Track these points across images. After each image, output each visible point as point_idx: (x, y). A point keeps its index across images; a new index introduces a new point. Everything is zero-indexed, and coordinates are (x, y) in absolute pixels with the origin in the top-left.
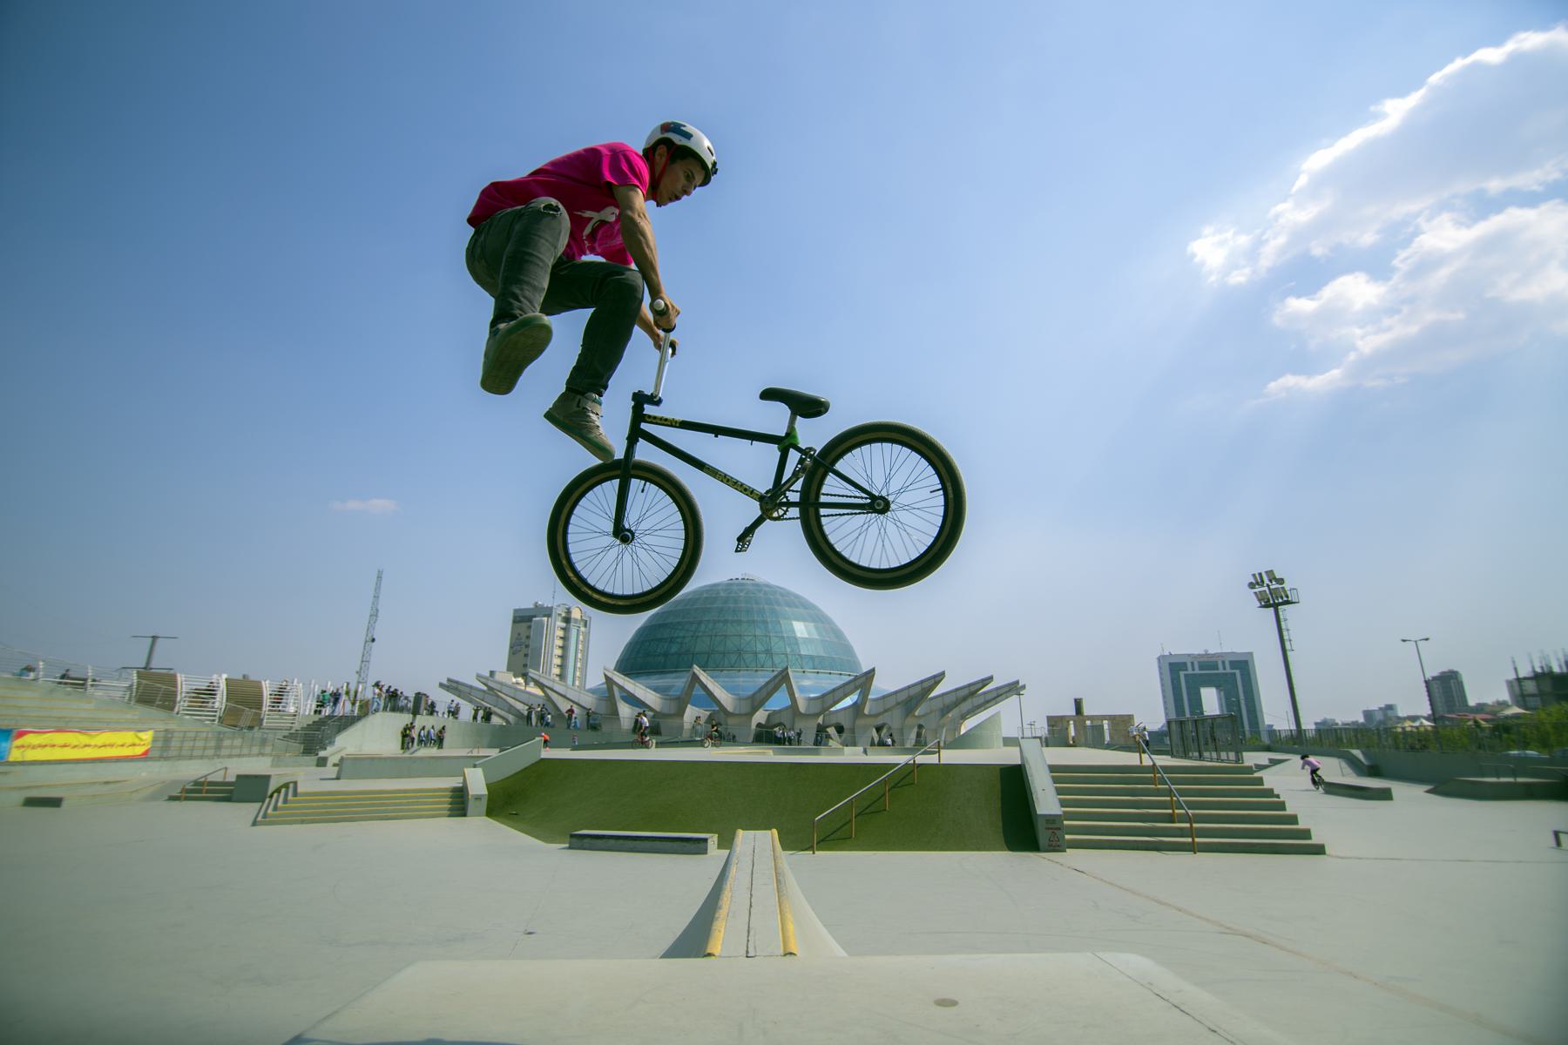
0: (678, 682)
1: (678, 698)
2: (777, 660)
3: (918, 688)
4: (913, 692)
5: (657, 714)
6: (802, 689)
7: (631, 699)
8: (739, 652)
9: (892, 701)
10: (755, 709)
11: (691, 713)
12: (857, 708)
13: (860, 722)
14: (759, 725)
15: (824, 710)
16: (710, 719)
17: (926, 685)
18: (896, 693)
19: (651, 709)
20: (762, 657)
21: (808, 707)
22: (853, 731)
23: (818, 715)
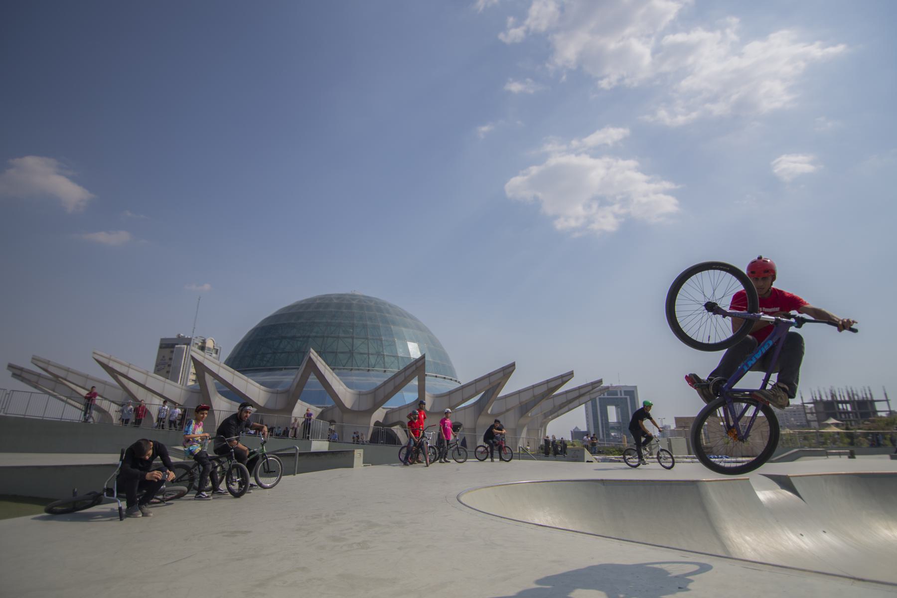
0: (288, 378)
1: (287, 392)
2: (386, 359)
5: (260, 409)
7: (231, 392)
8: (351, 353)
9: (515, 402)
11: (300, 409)
19: (253, 404)
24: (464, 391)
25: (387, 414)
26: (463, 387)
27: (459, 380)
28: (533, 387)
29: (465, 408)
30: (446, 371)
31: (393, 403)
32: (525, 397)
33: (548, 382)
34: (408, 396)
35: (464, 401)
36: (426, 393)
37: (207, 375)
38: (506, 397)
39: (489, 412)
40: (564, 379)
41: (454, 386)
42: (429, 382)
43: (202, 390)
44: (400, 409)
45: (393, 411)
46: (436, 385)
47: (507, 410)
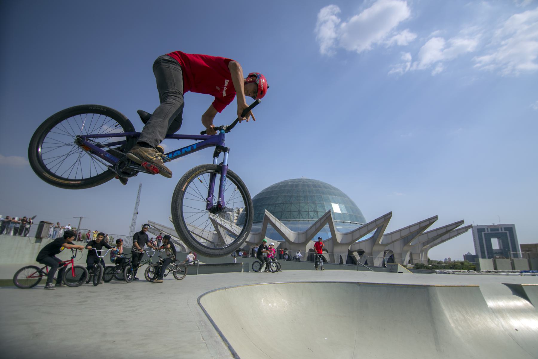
3: (417, 227)
4: (413, 230)
6: (338, 230)
9: (397, 236)
10: (307, 241)
12: (374, 240)
13: (376, 248)
14: (311, 250)
15: (352, 242)
16: (280, 246)
17: (423, 225)
18: (400, 230)
20: (312, 214)
21: (342, 240)
22: (371, 254)
23: (348, 244)
28: (410, 227)
29: (365, 241)
32: (404, 234)
33: (420, 223)
37: (219, 227)
38: (391, 234)
39: (380, 242)
43: (219, 234)
47: (393, 242)
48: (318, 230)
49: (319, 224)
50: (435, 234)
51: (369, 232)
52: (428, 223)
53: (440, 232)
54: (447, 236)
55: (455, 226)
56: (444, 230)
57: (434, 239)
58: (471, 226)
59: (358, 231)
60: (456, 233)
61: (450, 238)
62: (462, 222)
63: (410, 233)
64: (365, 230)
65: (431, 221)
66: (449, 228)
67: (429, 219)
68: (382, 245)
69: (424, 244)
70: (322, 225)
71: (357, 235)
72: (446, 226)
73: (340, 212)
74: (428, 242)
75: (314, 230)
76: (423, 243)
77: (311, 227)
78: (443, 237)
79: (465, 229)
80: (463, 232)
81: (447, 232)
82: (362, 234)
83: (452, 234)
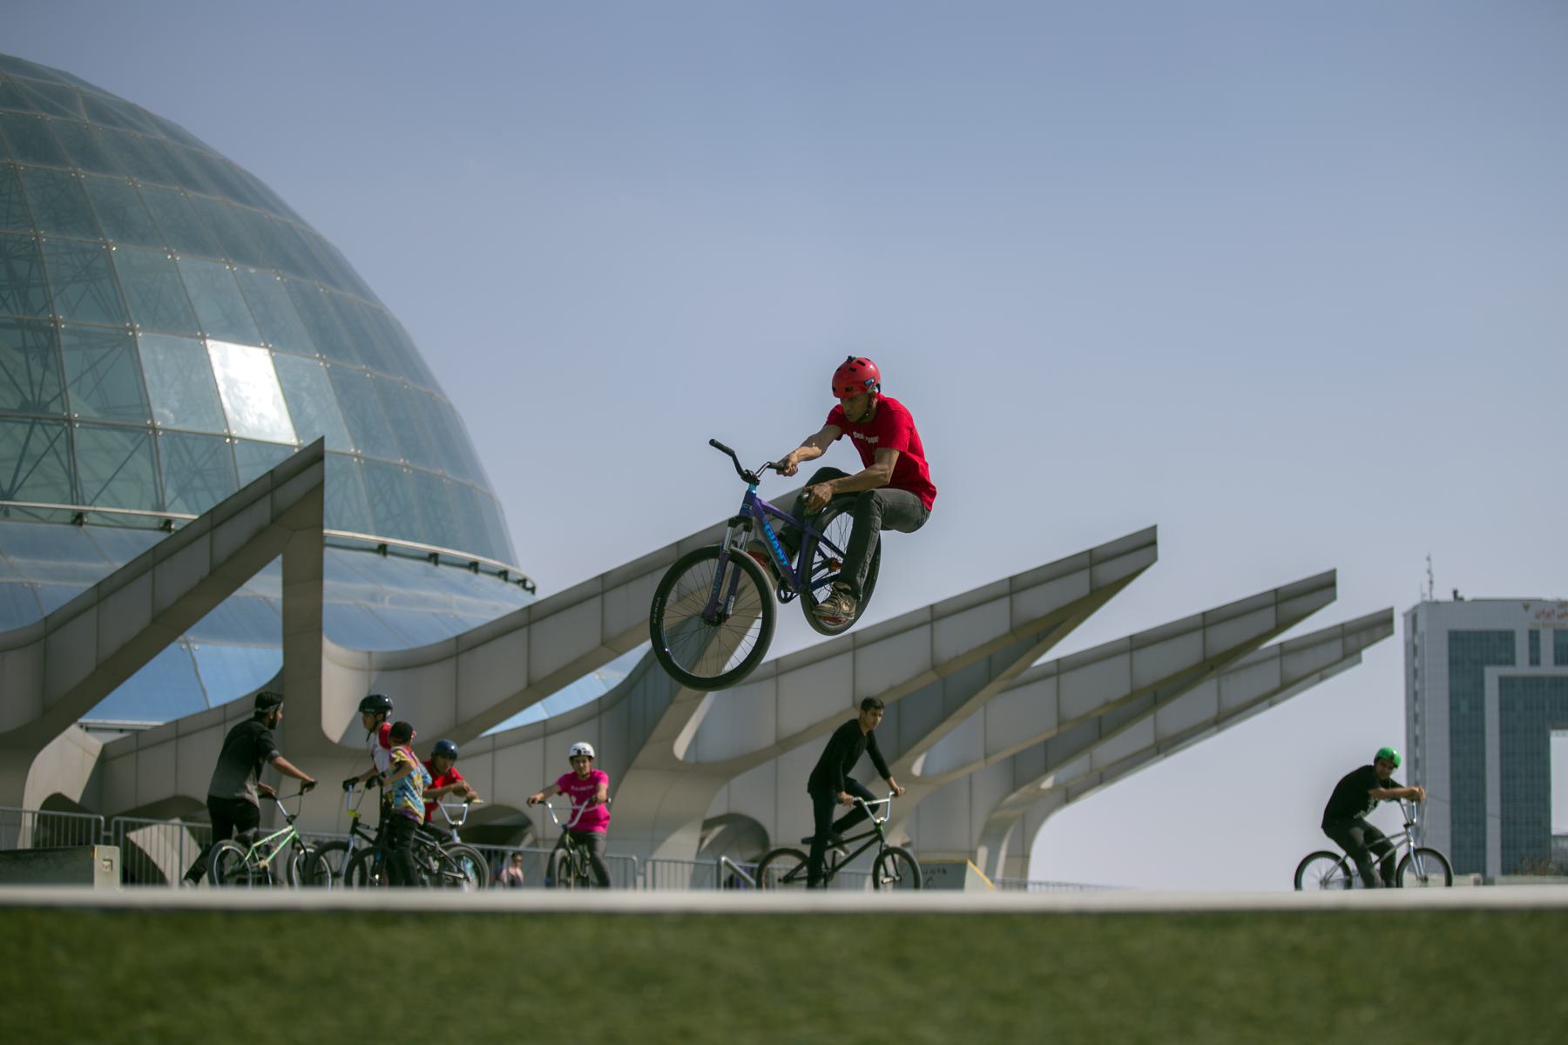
3: (994, 623)
4: (957, 639)
17: (1037, 604)
24: (544, 633)
25: (105, 760)
26: (532, 617)
27: (521, 569)
30: (448, 513)
31: (139, 705)
33: (1015, 586)
34: (225, 664)
35: (538, 689)
36: (328, 646)
39: (681, 747)
40: (1107, 573)
41: (494, 603)
42: (344, 588)
44: (178, 732)
45: (137, 742)
46: (384, 604)
48: (168, 625)
49: (195, 563)
50: (1113, 683)
51: (609, 648)
52: (1078, 586)
53: (1157, 665)
54: (1201, 700)
55: (1267, 619)
56: (1187, 653)
57: (1104, 725)
58: (1379, 625)
59: (516, 641)
60: (1268, 677)
61: (1222, 719)
62: (1322, 588)
63: (935, 666)
64: (580, 632)
65: (1107, 573)
66: (1224, 638)
67: (1092, 559)
68: (710, 771)
69: (1021, 770)
70: (225, 577)
71: (500, 671)
72: (1207, 621)
73: (293, 441)
74: (1051, 755)
75: (130, 616)
76: (1014, 760)
77: (105, 591)
78: (1173, 715)
79: (1336, 649)
80: (1321, 673)
81: (1213, 665)
82: (546, 666)
83: (1238, 686)
